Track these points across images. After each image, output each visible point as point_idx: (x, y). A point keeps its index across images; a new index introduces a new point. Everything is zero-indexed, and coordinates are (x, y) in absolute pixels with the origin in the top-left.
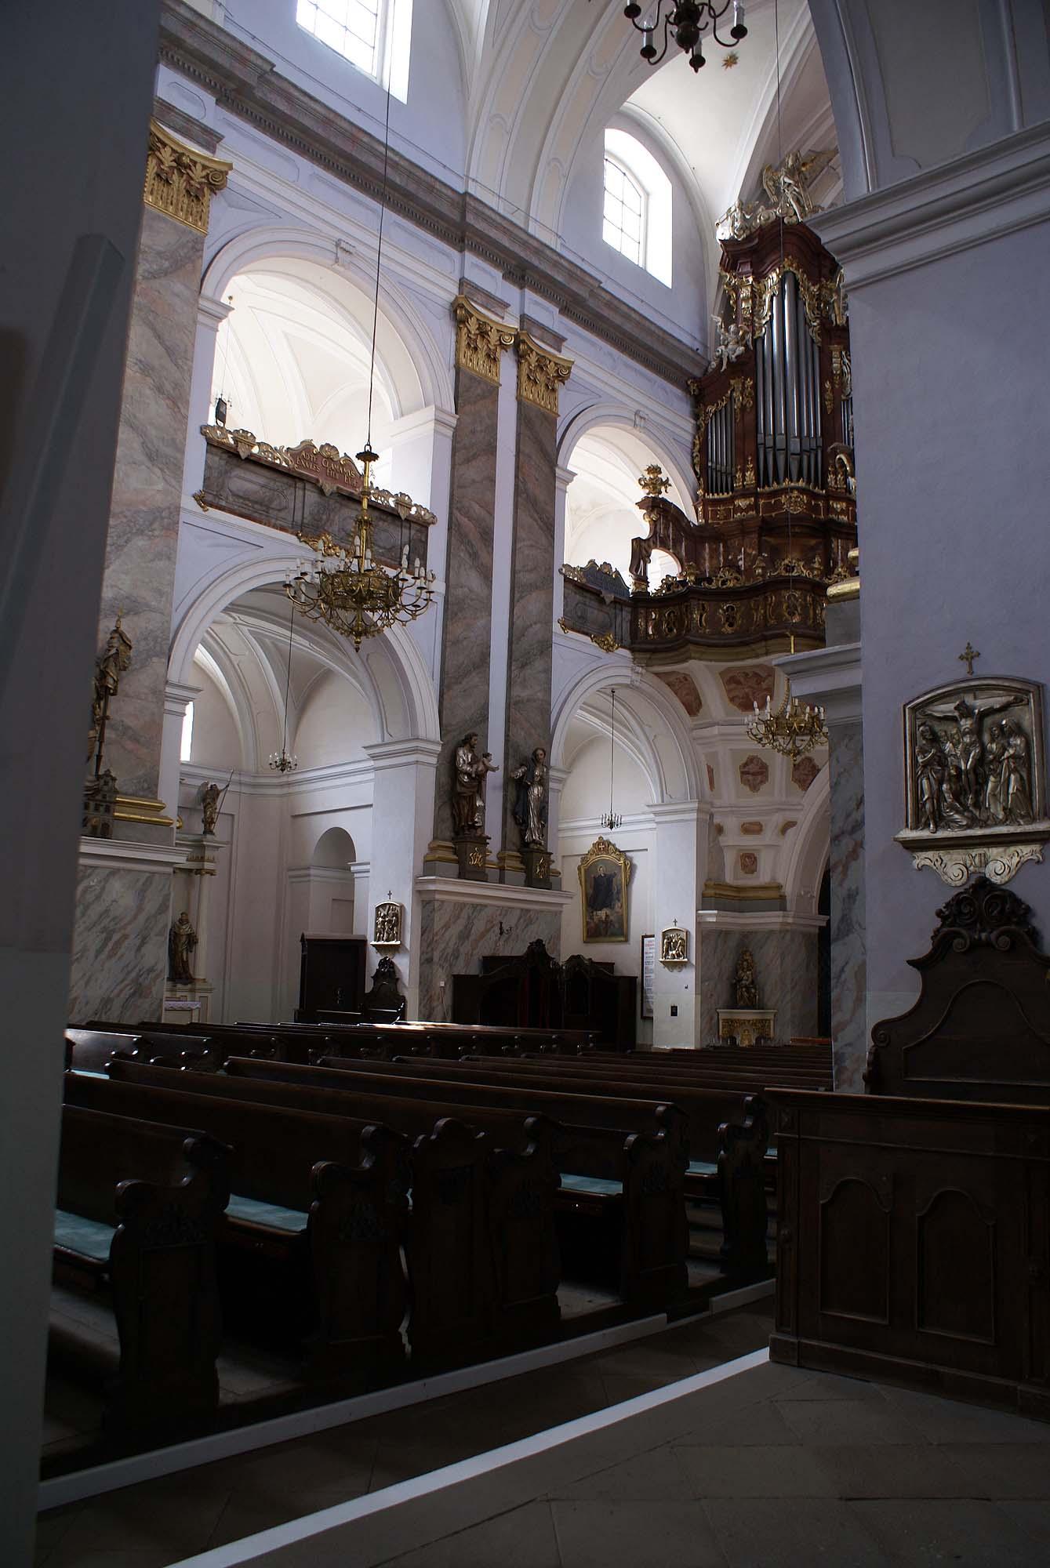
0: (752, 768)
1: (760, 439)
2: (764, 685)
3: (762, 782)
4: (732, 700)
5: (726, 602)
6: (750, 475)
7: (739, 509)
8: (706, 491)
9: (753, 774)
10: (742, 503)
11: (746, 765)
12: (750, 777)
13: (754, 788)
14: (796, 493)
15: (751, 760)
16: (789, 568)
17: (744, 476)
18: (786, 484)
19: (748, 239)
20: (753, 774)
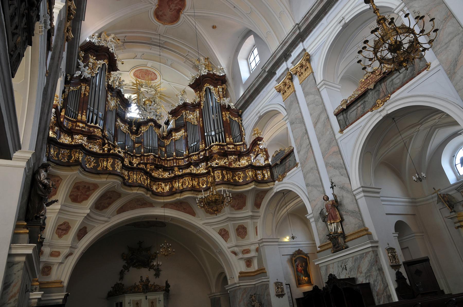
0: (63, 227)
1: (89, 106)
2: (88, 193)
3: (65, 234)
4: (70, 196)
5: (89, 155)
6: (84, 118)
7: (79, 126)
8: (65, 114)
9: (63, 230)
10: (81, 125)
11: (61, 225)
12: (60, 231)
13: (60, 236)
14: (100, 130)
15: (64, 223)
16: (119, 152)
17: (82, 116)
18: (98, 125)
19: (99, 46)
20: (63, 230)
